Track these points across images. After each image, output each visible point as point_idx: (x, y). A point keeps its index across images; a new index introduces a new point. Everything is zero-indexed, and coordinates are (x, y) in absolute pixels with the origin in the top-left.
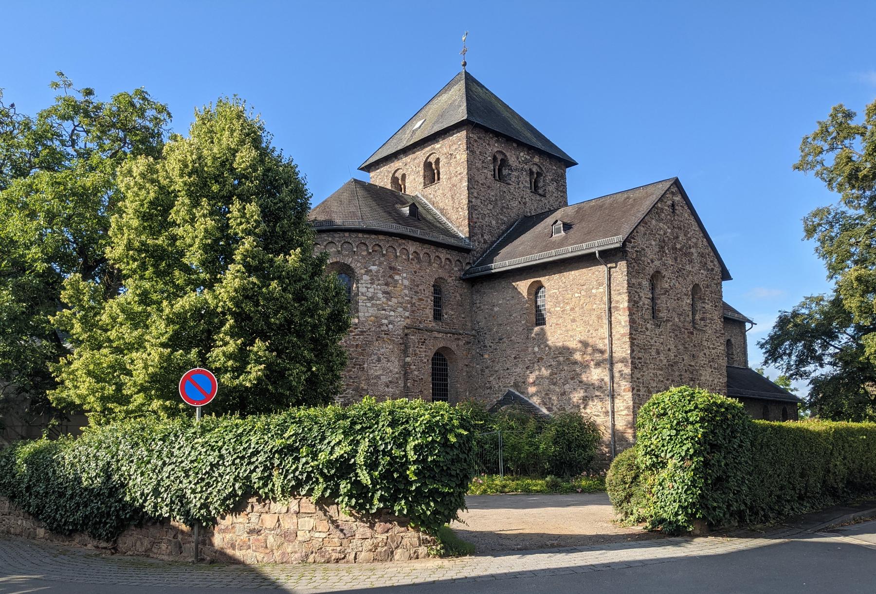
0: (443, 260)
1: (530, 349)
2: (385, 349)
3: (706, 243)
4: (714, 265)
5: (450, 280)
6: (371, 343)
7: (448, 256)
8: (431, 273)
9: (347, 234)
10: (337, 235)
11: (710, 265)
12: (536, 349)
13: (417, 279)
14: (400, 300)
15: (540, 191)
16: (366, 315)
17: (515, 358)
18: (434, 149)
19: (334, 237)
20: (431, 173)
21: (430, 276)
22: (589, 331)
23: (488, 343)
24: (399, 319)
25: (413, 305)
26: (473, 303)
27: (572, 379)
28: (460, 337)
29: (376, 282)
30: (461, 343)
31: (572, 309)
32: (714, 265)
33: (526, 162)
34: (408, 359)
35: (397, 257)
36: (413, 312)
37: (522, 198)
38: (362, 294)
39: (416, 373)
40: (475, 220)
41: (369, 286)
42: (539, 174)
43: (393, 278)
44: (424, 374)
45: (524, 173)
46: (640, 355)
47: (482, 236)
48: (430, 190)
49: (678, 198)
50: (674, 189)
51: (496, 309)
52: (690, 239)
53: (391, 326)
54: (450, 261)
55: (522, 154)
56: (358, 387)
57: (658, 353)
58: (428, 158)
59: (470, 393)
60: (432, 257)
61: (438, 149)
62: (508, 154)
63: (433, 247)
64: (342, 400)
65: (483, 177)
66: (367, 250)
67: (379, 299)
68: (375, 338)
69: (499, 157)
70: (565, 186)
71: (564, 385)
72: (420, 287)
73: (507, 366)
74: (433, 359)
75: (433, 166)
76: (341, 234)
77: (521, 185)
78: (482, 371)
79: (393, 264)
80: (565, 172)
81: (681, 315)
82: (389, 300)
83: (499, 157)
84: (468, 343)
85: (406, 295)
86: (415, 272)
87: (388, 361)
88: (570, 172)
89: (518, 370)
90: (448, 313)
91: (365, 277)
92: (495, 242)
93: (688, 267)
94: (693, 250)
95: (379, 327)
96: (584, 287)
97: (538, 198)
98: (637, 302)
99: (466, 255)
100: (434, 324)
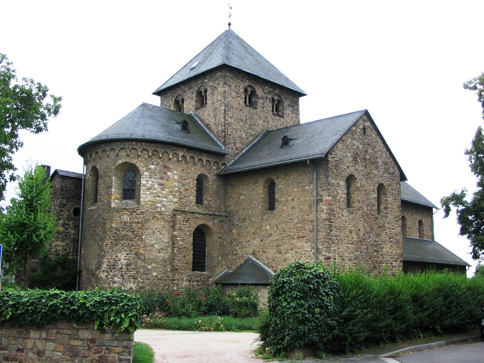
0: (204, 161)
1: (264, 227)
2: (158, 224)
3: (388, 155)
4: (395, 170)
5: (209, 176)
6: (148, 220)
7: (209, 159)
8: (195, 171)
9: (134, 143)
10: (127, 143)
11: (391, 170)
12: (268, 227)
13: (184, 175)
15: (280, 114)
16: (145, 200)
17: (254, 233)
18: (203, 82)
19: (125, 145)
20: (202, 99)
21: (194, 172)
22: (303, 216)
23: (236, 222)
24: (169, 203)
25: (181, 193)
26: (226, 193)
27: (291, 249)
28: (215, 217)
29: (154, 177)
30: (216, 221)
31: (293, 200)
32: (395, 170)
33: (269, 93)
34: (175, 233)
35: (170, 159)
36: (180, 198)
37: (266, 117)
38: (144, 185)
39: (181, 243)
40: (229, 133)
41: (148, 179)
42: (279, 102)
43: (166, 174)
44: (187, 244)
45: (268, 101)
46: (337, 234)
47: (235, 144)
48: (199, 111)
49: (368, 124)
50: (365, 118)
51: (242, 197)
52: (376, 152)
53: (163, 209)
55: (266, 88)
56: (138, 252)
57: (351, 232)
58: (199, 88)
59: (222, 258)
60: (196, 159)
61: (206, 82)
62: (256, 88)
63: (197, 152)
65: (237, 103)
66: (149, 154)
67: (155, 189)
68: (151, 218)
69: (249, 90)
70: (298, 110)
71: (286, 253)
72: (187, 181)
73: (249, 239)
74: (194, 233)
75: (203, 94)
76: (131, 143)
77: (265, 109)
78: (231, 242)
80: (298, 100)
81: (368, 205)
83: (249, 90)
84: (222, 221)
85: (176, 186)
86: (183, 170)
87: (161, 234)
88: (301, 99)
89: (255, 242)
90: (207, 199)
91: (146, 173)
92: (244, 148)
93: (375, 172)
94: (379, 160)
95: (155, 209)
96: (301, 184)
97: (278, 118)
98: (336, 197)
99: (222, 158)
100: (196, 208)
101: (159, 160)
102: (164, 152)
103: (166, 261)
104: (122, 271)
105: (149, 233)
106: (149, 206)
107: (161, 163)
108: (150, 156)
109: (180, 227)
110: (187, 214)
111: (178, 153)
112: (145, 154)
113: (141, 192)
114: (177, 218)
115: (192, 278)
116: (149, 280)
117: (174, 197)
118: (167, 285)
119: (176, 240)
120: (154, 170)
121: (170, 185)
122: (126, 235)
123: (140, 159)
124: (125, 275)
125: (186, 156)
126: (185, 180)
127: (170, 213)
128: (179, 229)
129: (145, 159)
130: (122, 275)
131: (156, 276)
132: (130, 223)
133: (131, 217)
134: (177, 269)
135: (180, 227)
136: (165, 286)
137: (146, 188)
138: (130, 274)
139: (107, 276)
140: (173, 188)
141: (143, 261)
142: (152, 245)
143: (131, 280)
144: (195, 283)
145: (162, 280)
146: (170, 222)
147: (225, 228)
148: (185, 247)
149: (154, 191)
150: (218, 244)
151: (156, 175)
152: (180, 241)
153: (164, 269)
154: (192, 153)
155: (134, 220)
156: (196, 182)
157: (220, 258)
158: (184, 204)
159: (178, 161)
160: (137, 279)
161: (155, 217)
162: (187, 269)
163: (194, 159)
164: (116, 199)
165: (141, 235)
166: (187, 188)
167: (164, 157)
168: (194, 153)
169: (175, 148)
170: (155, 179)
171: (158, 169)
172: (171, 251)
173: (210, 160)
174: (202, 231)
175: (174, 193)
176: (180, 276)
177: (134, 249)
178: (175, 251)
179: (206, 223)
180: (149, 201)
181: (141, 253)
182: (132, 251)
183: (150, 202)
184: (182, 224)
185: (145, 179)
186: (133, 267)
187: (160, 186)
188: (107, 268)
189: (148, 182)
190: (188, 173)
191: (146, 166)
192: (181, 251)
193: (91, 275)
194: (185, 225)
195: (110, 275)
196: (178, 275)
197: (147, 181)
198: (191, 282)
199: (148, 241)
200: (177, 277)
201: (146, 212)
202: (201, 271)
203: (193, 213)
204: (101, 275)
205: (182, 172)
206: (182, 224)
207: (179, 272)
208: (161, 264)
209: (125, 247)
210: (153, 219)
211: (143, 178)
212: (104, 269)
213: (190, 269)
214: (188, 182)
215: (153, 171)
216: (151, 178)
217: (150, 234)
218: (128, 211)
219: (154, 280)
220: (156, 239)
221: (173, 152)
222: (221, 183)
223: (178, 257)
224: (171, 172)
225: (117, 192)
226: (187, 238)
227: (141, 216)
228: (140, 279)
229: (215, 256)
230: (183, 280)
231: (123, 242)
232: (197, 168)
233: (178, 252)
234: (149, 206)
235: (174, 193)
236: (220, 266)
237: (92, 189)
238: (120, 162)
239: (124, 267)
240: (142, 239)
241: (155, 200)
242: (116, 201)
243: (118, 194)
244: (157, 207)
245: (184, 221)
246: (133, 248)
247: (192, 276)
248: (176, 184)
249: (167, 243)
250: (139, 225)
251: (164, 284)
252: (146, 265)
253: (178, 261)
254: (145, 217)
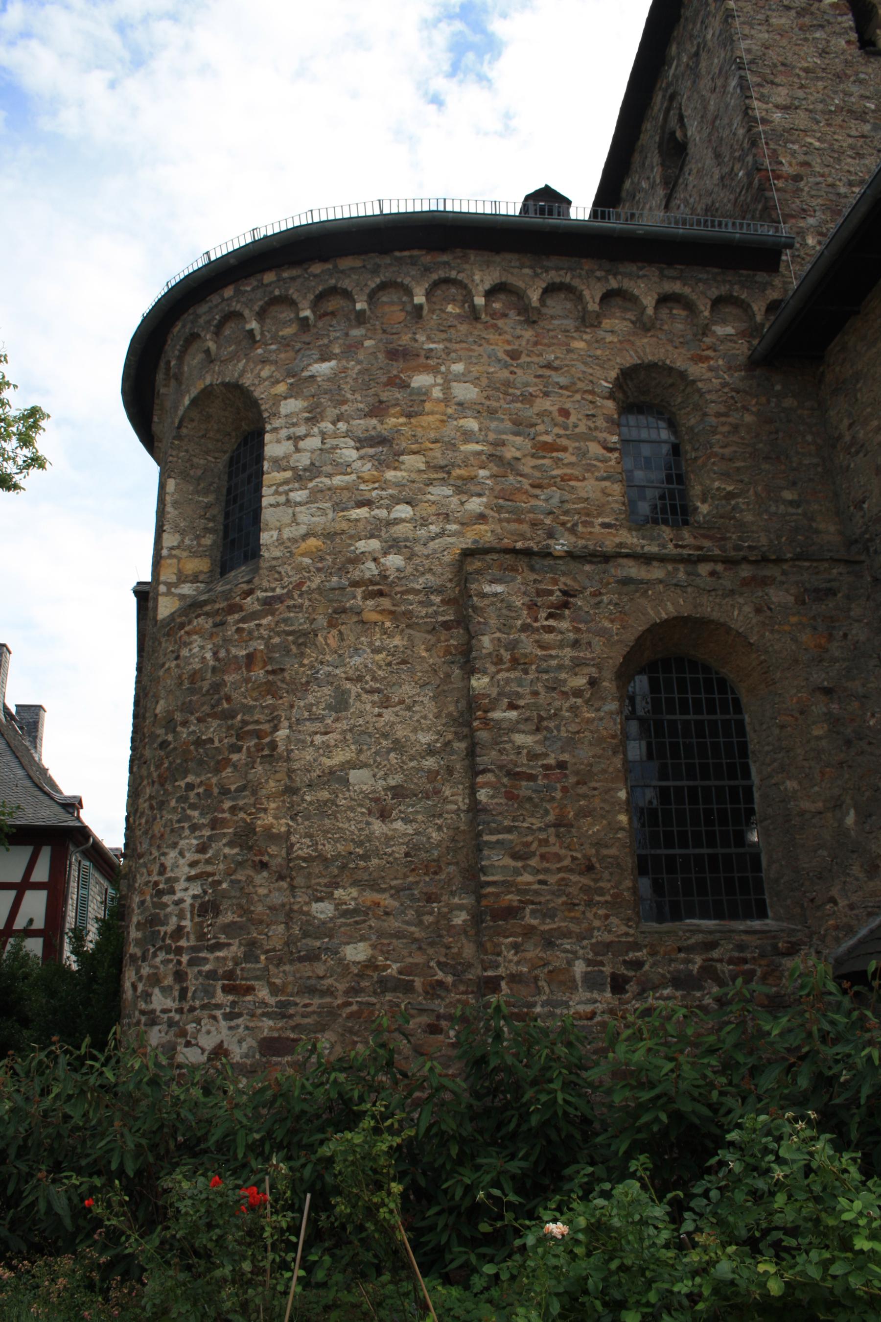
5: (695, 370)
6: (305, 638)
14: (438, 455)
16: (287, 533)
29: (332, 412)
30: (778, 596)
34: (479, 683)
41: (301, 430)
43: (405, 386)
44: (570, 743)
53: (394, 561)
54: (689, 306)
56: (250, 829)
59: (864, 816)
64: (196, 889)
67: (345, 468)
68: (322, 621)
79: (405, 339)
82: (393, 461)
85: (468, 436)
86: (514, 355)
87: (385, 703)
91: (291, 406)
95: (342, 570)
101: (356, 332)
102: (383, 287)
103: (433, 868)
104: (179, 951)
105: (309, 708)
106: (307, 561)
107: (367, 343)
108: (304, 324)
109: (512, 646)
110: (552, 569)
111: (460, 277)
112: (286, 323)
113: (265, 502)
114: (484, 596)
115: (638, 964)
116: (324, 993)
117: (459, 490)
118: (450, 1018)
119: (486, 723)
120: (329, 380)
121: (433, 435)
122: (199, 743)
123: (260, 351)
124: (192, 972)
125: (521, 284)
126: (528, 399)
127: (440, 576)
128: (499, 661)
129: (286, 344)
130: (180, 976)
131: (370, 965)
132: (214, 669)
133: (218, 640)
134: (511, 912)
135: (512, 646)
136: (434, 1029)
137: (288, 474)
138: (211, 961)
140: (452, 446)
141: (281, 878)
142: (336, 777)
143: (220, 997)
144: (666, 1000)
145: (408, 988)
146: (446, 625)
147: (859, 632)
148: (562, 765)
149: (338, 480)
150: (818, 731)
151: (345, 402)
152: (514, 728)
153: (419, 914)
154: (558, 269)
155: (234, 651)
156: (610, 404)
157: (850, 819)
158: (534, 524)
159: (474, 315)
160: (250, 990)
161: (344, 611)
162: (590, 904)
163: (580, 298)
164: (182, 578)
165: (266, 727)
166: (548, 439)
167: (387, 309)
168: (570, 269)
169: (445, 258)
170: (339, 418)
171: (353, 373)
172: (462, 802)
173: (687, 290)
174: (707, 669)
175: (457, 472)
176: (533, 952)
177: (233, 810)
178: (483, 795)
179: (709, 608)
180: (305, 537)
181: (268, 829)
182: (223, 823)
183: (312, 542)
184: (525, 628)
185: (284, 433)
186: (229, 917)
187: (371, 451)
189: (301, 444)
190: (549, 366)
191: (291, 374)
192: (525, 789)
194: (550, 630)
196: (516, 947)
197: (296, 439)
198: (632, 988)
199: (309, 755)
200: (510, 962)
201: (289, 595)
202: (734, 916)
203: (606, 558)
205: (506, 366)
206: (525, 628)
207: (529, 932)
208: (398, 890)
209: (193, 807)
210: (332, 625)
211: (275, 430)
213: (615, 904)
214: (554, 409)
215: (326, 385)
216: (312, 420)
217: (318, 711)
218: (207, 614)
219: (354, 991)
220: (359, 735)
221: (435, 277)
222: (789, 402)
223: (509, 830)
224: (434, 370)
225: (189, 548)
226: (573, 709)
227: (267, 620)
228: (263, 993)
229: (806, 805)
230: (561, 979)
231: (182, 784)
232: (609, 338)
233: (510, 796)
234: (307, 561)
235: (457, 472)
236: (856, 870)
238: (187, 401)
239: (187, 923)
240: (273, 745)
241: (344, 525)
242: (187, 589)
243: (194, 554)
244: (357, 560)
245: (532, 607)
246: (227, 805)
247: (636, 946)
248: (472, 424)
249: (431, 752)
250: (259, 674)
251: (424, 1019)
252: (301, 898)
253: (515, 856)
254: (285, 620)
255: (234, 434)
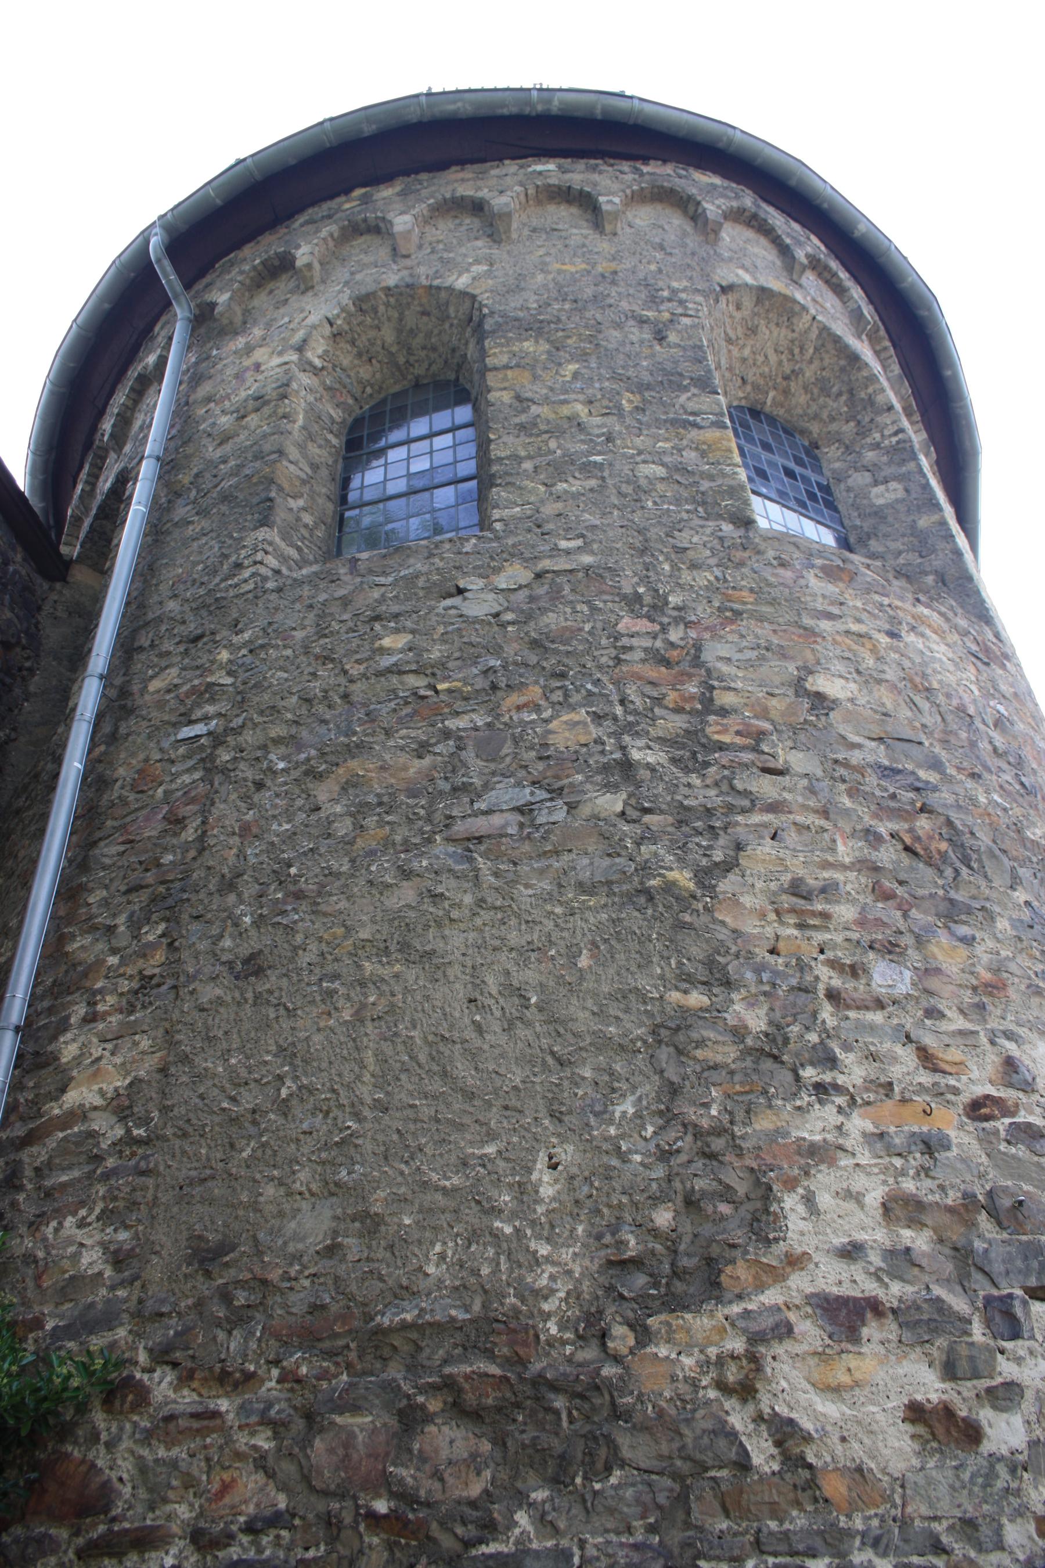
139: (943, 1428)
188: (901, 1260)
193: (448, 1439)
195: (1004, 1396)
204: (793, 1385)
212: (831, 1277)
237: (315, 467)
255: (749, 388)
